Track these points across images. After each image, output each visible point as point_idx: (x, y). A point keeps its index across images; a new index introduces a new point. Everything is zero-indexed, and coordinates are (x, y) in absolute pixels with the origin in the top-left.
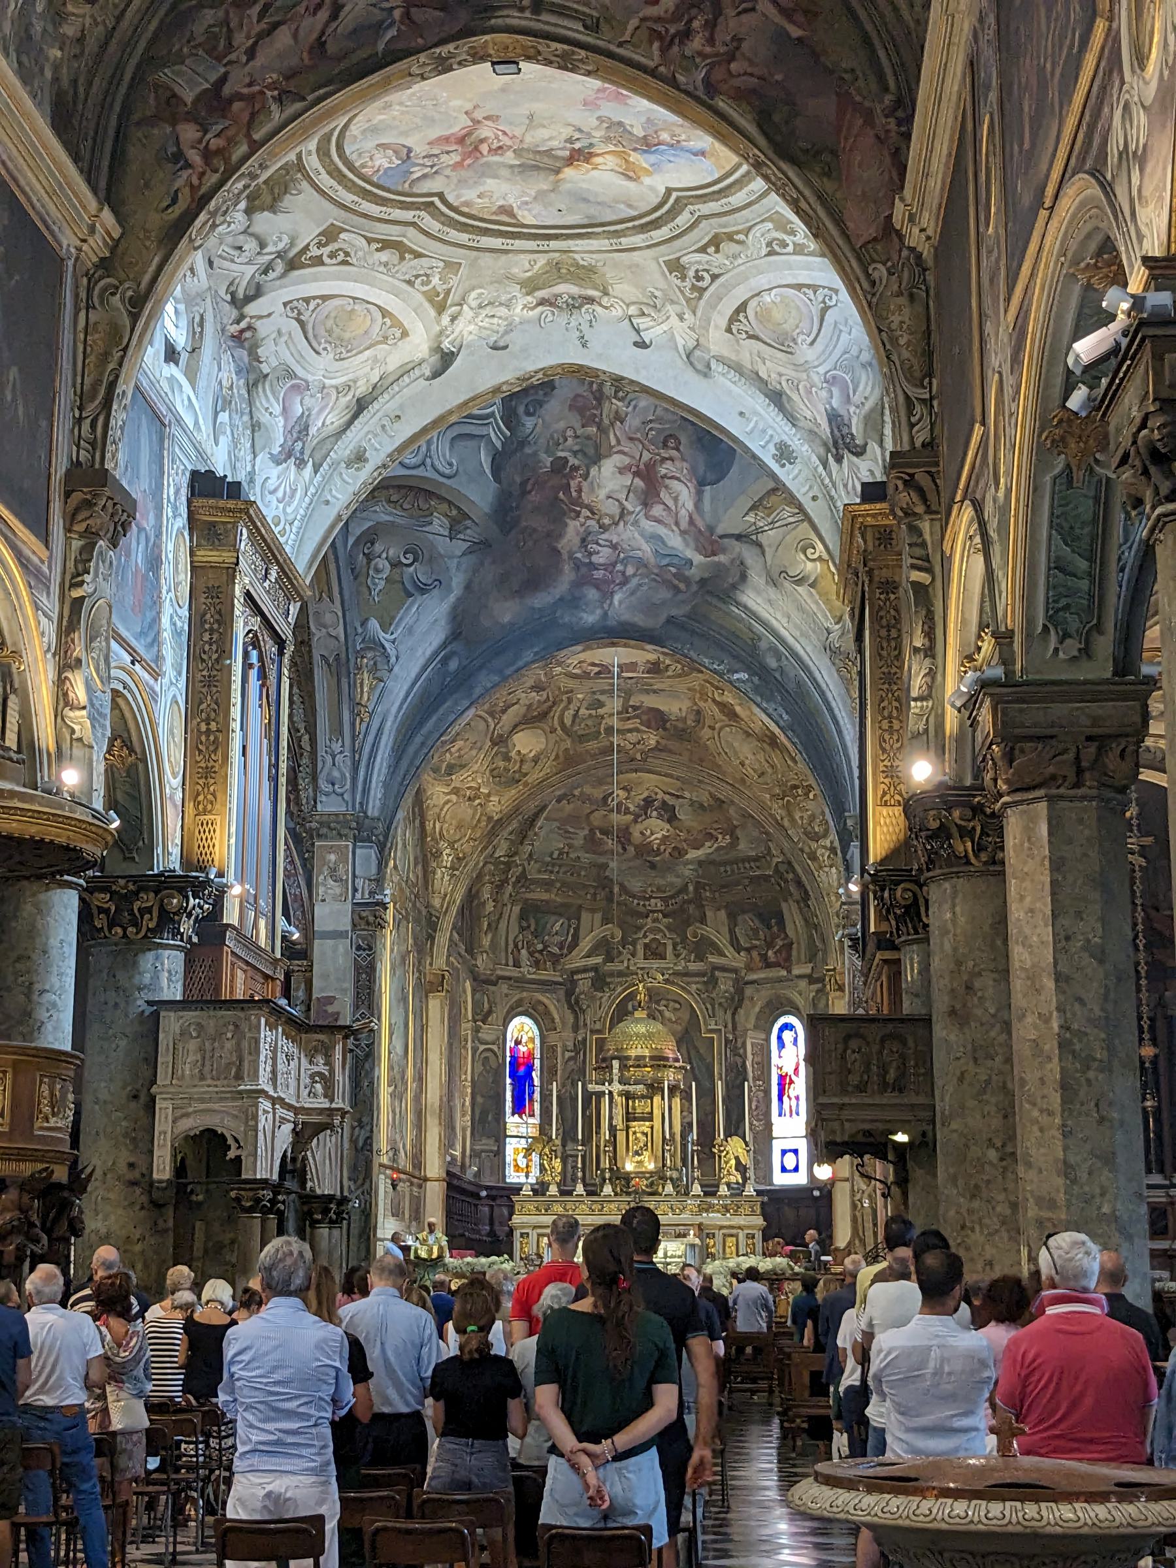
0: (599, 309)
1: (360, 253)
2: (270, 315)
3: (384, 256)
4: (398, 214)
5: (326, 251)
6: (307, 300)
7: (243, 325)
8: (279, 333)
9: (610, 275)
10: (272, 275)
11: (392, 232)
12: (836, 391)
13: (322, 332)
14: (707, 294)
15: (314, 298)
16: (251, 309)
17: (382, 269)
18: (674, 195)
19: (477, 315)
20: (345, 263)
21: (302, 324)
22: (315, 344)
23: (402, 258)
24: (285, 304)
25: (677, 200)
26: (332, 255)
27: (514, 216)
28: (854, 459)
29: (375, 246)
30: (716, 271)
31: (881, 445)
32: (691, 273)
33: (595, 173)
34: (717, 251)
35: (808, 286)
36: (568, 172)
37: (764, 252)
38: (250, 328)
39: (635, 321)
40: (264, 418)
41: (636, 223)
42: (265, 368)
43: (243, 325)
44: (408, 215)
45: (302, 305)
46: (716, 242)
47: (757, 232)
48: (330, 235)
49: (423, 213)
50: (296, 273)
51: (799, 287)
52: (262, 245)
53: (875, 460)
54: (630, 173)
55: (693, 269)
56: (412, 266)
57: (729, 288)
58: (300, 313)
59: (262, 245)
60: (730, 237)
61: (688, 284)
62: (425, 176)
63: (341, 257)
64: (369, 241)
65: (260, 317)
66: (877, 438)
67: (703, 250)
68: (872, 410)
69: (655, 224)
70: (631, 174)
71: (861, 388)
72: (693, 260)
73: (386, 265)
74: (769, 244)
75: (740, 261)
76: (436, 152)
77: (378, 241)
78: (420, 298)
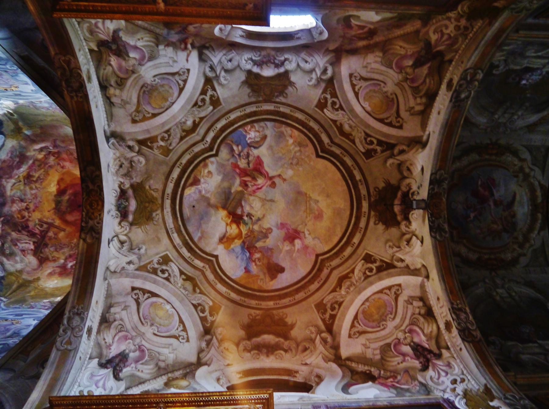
0: (118, 220)
1: (196, 113)
2: (187, 60)
3: (189, 123)
4: (211, 135)
5: (207, 98)
6: (185, 81)
7: (189, 46)
8: (175, 61)
9: (149, 227)
10: (208, 70)
11: (201, 130)
12: (137, 353)
13: (164, 82)
14: (154, 276)
15: (184, 85)
16: (194, 55)
17: (183, 120)
18: (214, 259)
19: (126, 159)
20: (196, 104)
21: (173, 74)
22: (158, 77)
23: (184, 131)
24: (188, 70)
25: (211, 261)
26: (203, 100)
27: (192, 185)
28: (112, 376)
29: (197, 120)
30: (172, 280)
32: (164, 267)
33: (224, 224)
34: (183, 279)
35: (184, 326)
36: (223, 213)
37: (194, 302)
38: (186, 48)
39: (115, 239)
40: (139, 36)
41: (189, 241)
42: (161, 47)
43: (189, 46)
44: (209, 139)
45: (184, 77)
46: (188, 278)
47: (204, 297)
48: (215, 102)
49: (207, 145)
50: (202, 81)
51: (181, 321)
52: (227, 71)
54: (225, 240)
55: (168, 268)
56: (177, 134)
57: (163, 286)
58: (180, 75)
59: (227, 71)
60: (195, 286)
61: (156, 266)
62: (232, 150)
63: (200, 103)
64: (201, 119)
65: (188, 56)
66: (128, 384)
67: (182, 273)
68: (139, 378)
69: (190, 250)
70: (225, 240)
71: (146, 367)
72: (174, 268)
73: (185, 123)
74: (199, 305)
75: (183, 291)
76: (251, 158)
77: (199, 123)
78: (154, 134)
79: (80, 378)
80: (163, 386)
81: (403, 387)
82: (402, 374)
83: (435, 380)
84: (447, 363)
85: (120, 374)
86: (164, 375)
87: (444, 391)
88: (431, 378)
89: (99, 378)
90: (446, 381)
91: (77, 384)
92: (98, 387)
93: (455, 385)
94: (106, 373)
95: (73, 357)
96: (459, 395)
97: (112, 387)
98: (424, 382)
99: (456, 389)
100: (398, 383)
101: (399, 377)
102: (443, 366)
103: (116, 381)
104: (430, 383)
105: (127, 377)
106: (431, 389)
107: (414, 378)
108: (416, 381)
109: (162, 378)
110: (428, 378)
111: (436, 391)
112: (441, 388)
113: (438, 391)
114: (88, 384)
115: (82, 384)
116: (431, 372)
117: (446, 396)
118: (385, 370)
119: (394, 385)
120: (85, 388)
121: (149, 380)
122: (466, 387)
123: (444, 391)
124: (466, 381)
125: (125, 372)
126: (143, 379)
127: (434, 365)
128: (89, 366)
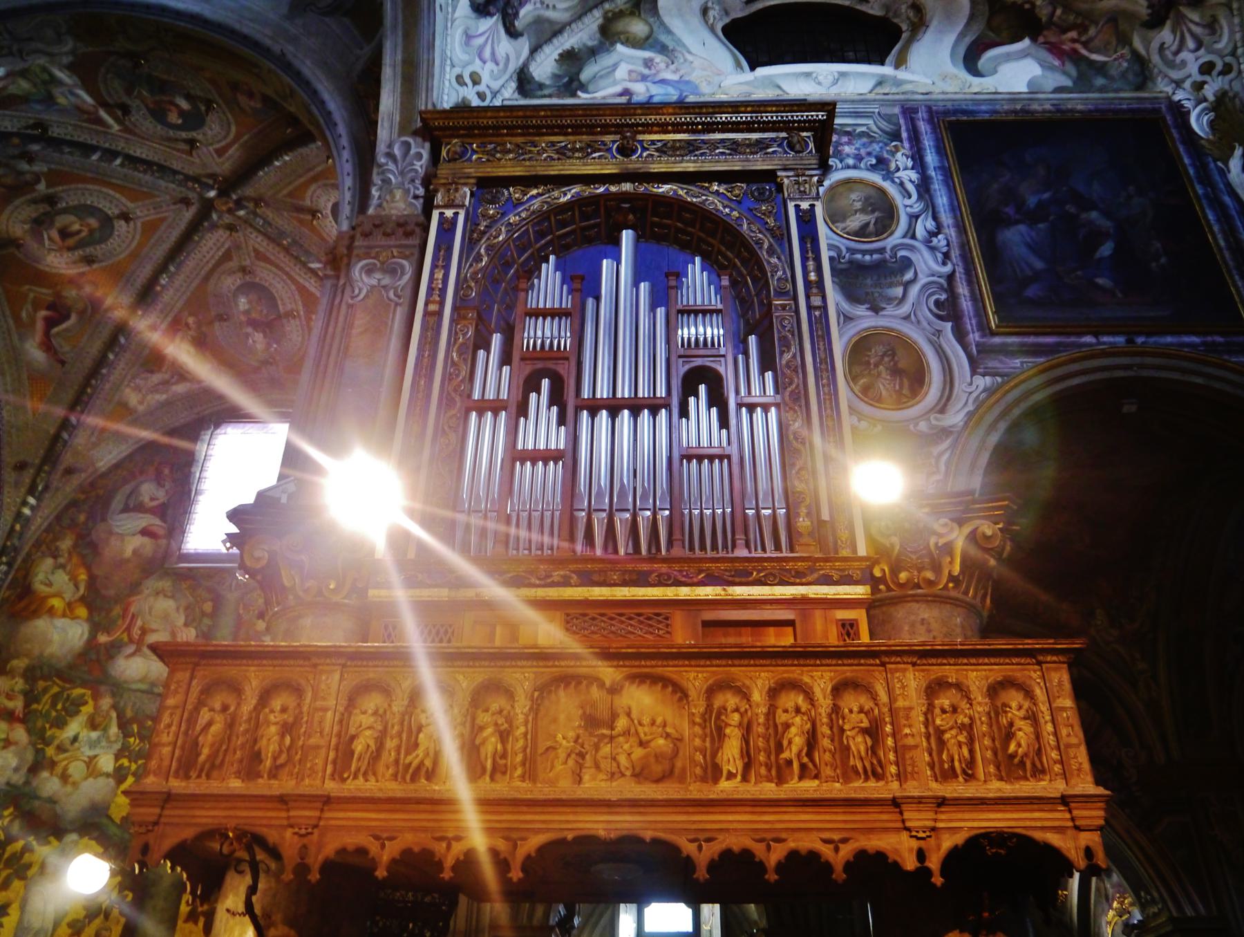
28: (502, 31)
31: (534, 50)
53: (518, 57)
68: (549, 21)
79: (449, 47)
80: (598, 35)
81: (1095, 57)
82: (1101, 23)
83: (1168, 53)
84: (1208, 20)
85: (517, 23)
86: (596, 6)
87: (1178, 84)
88: (1162, 48)
89: (480, 41)
90: (1191, 62)
91: (448, 62)
92: (485, 62)
93: (1207, 78)
94: (490, 28)
95: (429, 12)
96: (1205, 100)
97: (507, 55)
98: (1143, 52)
99: (1206, 86)
100: (1085, 45)
101: (1092, 31)
102: (1197, 24)
103: (512, 41)
104: (1156, 58)
105: (529, 25)
106: (1151, 72)
107: (1125, 40)
108: (1127, 47)
109: (594, 17)
110: (1155, 45)
111: (1163, 79)
112: (1175, 75)
113: (1166, 80)
114: (465, 57)
115: (455, 60)
116: (1166, 35)
117: (1179, 96)
118: (1067, 9)
119: (1075, 51)
120: (464, 67)
121: (570, 24)
122: (1227, 87)
123: (1178, 84)
124: (1232, 75)
125: (524, 17)
126: (558, 23)
127: (1180, 20)
128: (457, 15)
